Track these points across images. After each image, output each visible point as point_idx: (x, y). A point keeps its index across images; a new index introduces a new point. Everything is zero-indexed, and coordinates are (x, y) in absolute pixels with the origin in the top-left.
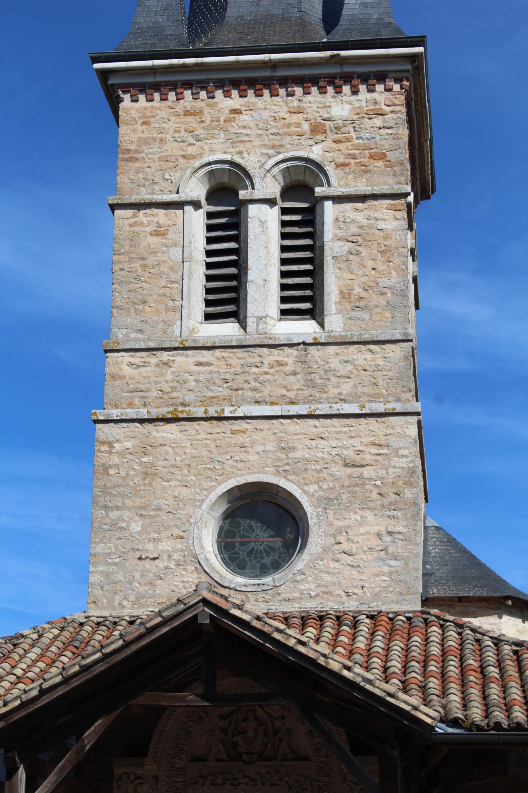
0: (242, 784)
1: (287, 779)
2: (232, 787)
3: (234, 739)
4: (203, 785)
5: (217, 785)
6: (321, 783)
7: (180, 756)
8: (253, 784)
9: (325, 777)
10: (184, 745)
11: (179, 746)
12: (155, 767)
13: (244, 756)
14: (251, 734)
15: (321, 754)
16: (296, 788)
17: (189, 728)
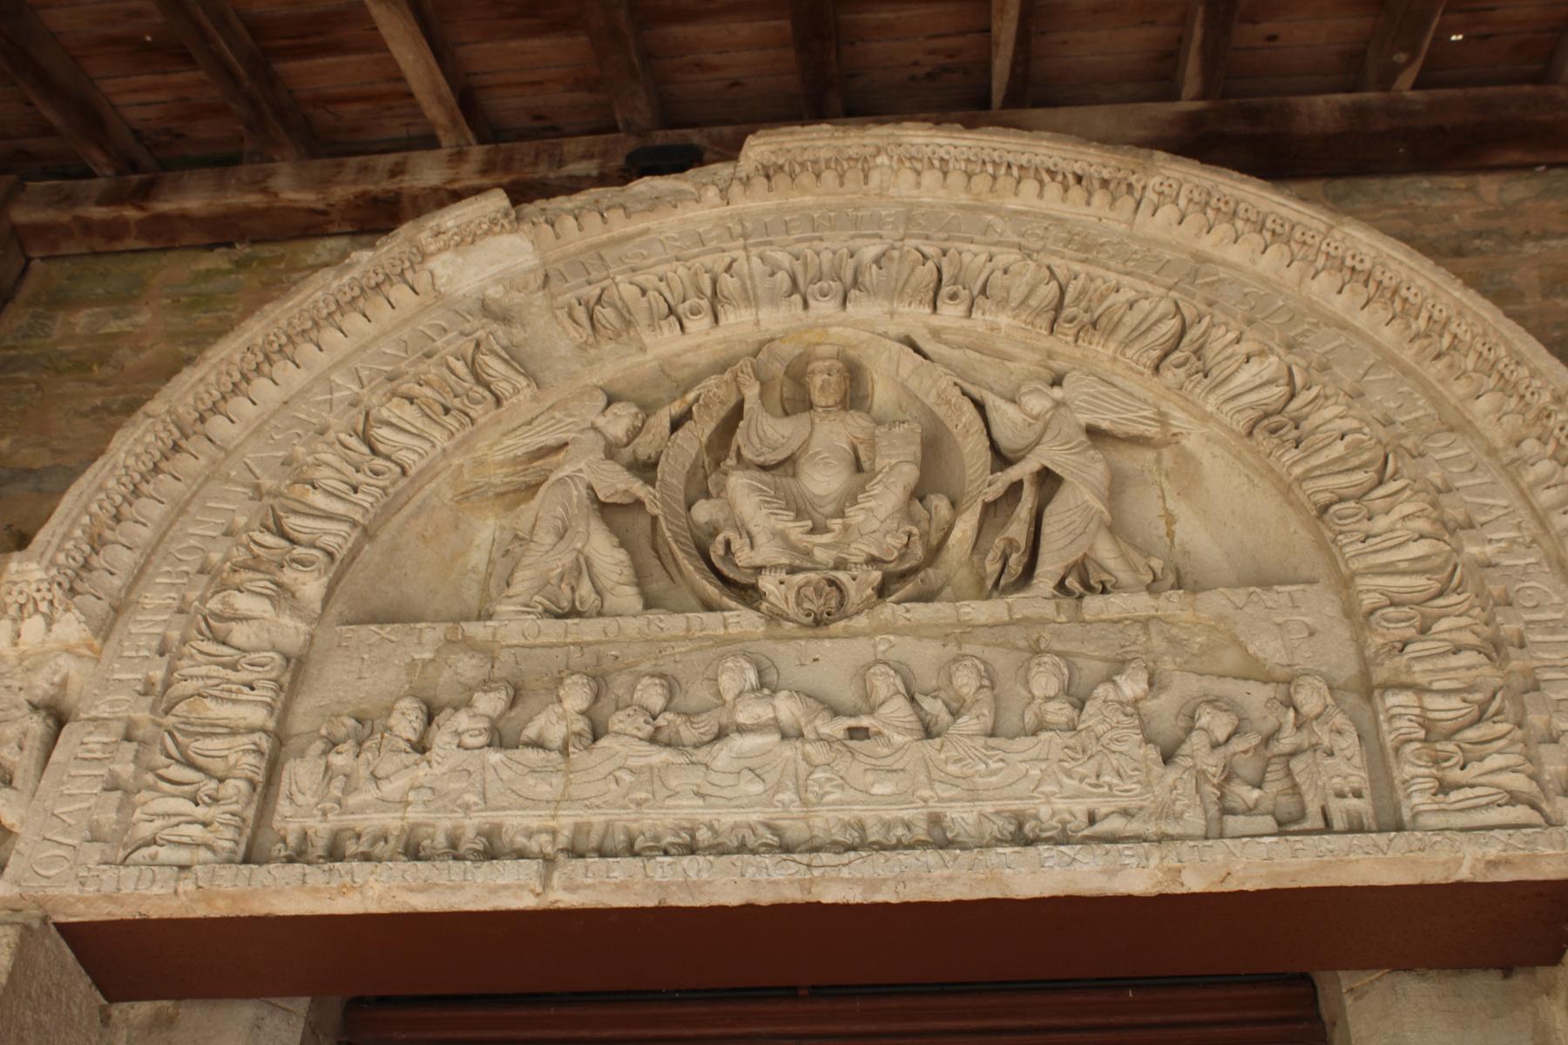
0: (741, 730)
1: (1132, 685)
2: (660, 756)
3: (703, 512)
4: (421, 747)
5: (538, 744)
6: (1432, 702)
7: (288, 575)
8: (838, 727)
9: (1468, 658)
10: (330, 517)
11: (292, 522)
12: (71, 628)
13: (767, 583)
14: (822, 481)
15: (1381, 523)
16: (1215, 746)
17: (384, 432)
